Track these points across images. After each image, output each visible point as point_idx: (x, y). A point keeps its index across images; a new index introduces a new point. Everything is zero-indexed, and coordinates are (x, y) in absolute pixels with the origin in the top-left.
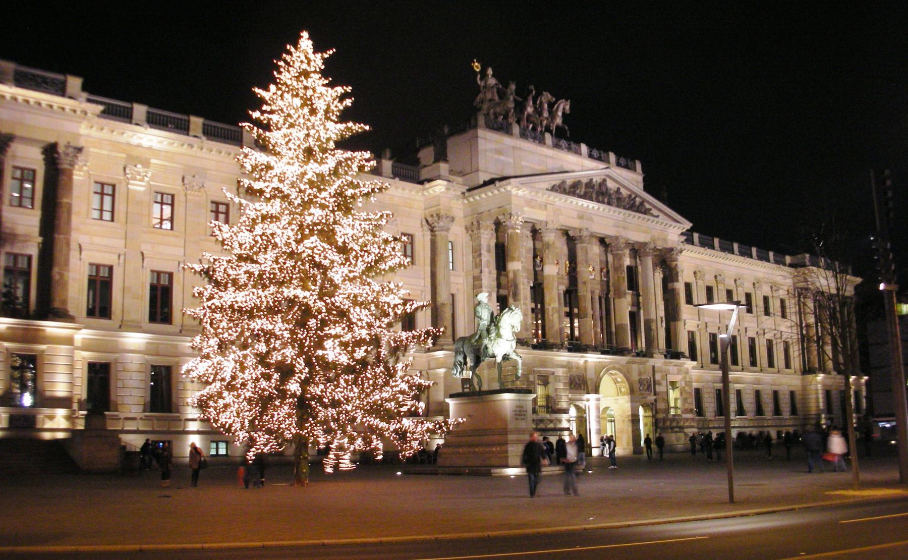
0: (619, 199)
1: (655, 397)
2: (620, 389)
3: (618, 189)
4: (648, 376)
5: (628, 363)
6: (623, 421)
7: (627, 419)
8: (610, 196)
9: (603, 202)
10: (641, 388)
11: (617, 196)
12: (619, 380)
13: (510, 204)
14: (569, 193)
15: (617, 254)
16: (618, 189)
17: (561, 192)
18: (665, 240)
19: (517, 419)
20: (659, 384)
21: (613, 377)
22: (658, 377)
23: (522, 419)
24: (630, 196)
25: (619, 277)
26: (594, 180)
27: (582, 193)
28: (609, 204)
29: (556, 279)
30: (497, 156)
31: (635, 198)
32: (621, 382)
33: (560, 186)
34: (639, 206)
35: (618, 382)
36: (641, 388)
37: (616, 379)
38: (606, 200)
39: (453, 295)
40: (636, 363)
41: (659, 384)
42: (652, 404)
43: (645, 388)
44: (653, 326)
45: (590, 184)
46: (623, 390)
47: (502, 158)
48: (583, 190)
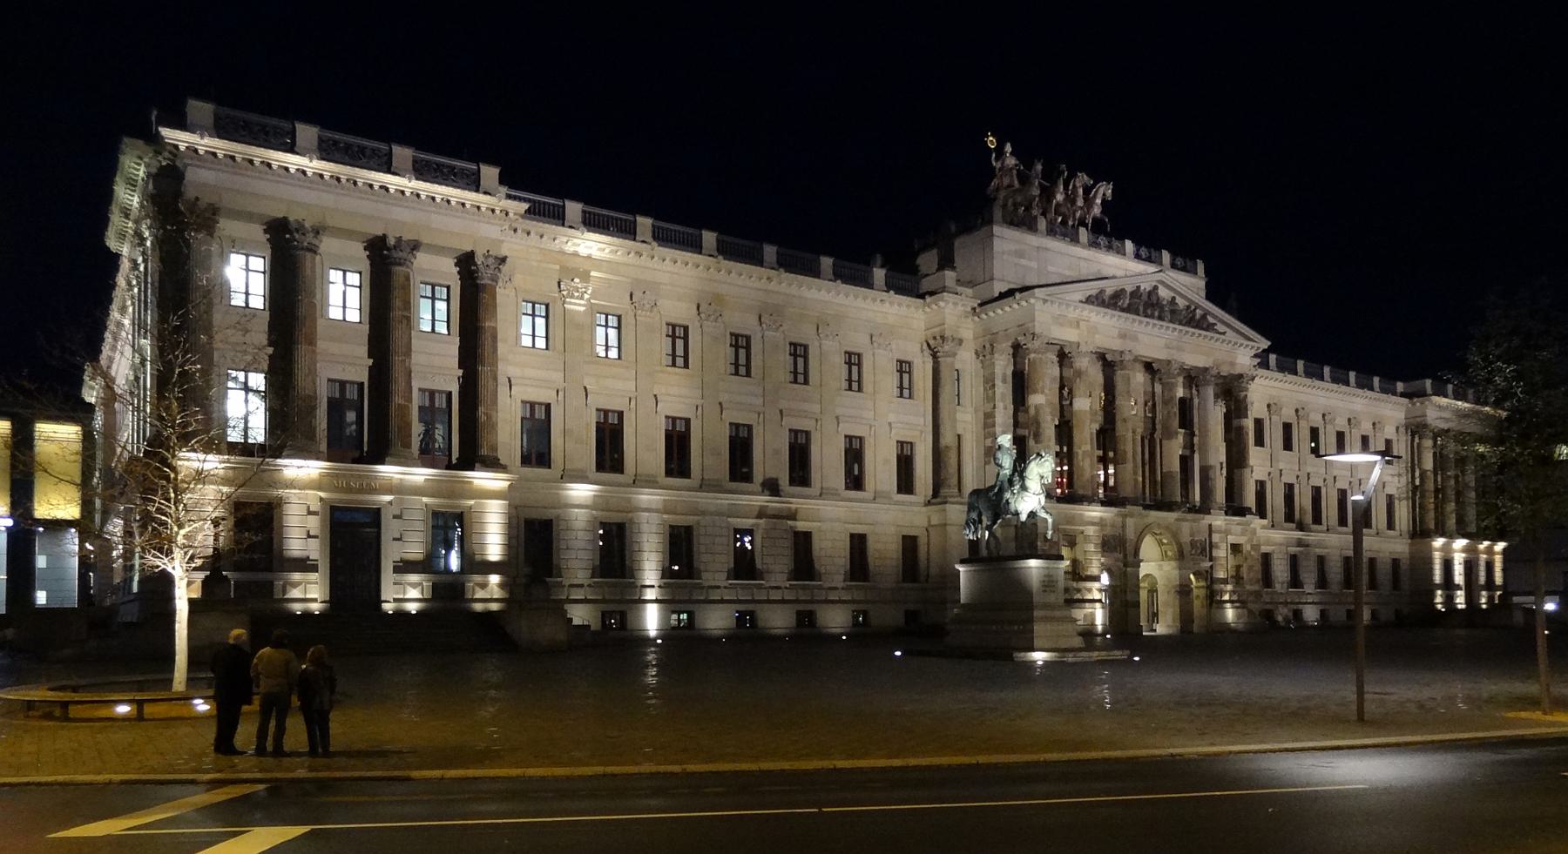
0: (1173, 312)
1: (1211, 563)
2: (1166, 552)
3: (1174, 298)
4: (1204, 536)
5: (1177, 520)
6: (1168, 593)
7: (1174, 590)
8: (1162, 308)
9: (1152, 316)
10: (1193, 552)
11: (1171, 308)
12: (1165, 541)
13: (1033, 321)
14: (1108, 307)
15: (1168, 383)
16: (1174, 298)
17: (1098, 305)
18: (1232, 364)
19: (1045, 591)
20: (1217, 547)
21: (1158, 537)
22: (1216, 538)
23: (1051, 591)
24: (1188, 307)
25: (1169, 413)
26: (1142, 288)
27: (1125, 305)
28: (1161, 318)
29: (1088, 416)
30: (1016, 260)
31: (1195, 310)
32: (1167, 544)
33: (1097, 297)
34: (1199, 320)
35: (1163, 544)
36: (1193, 552)
37: (1161, 540)
38: (1156, 314)
39: (959, 436)
40: (1187, 520)
41: (1217, 547)
42: (1207, 572)
43: (1199, 551)
44: (1211, 474)
45: (1136, 293)
46: (1169, 553)
47: (1023, 262)
48: (1127, 301)
